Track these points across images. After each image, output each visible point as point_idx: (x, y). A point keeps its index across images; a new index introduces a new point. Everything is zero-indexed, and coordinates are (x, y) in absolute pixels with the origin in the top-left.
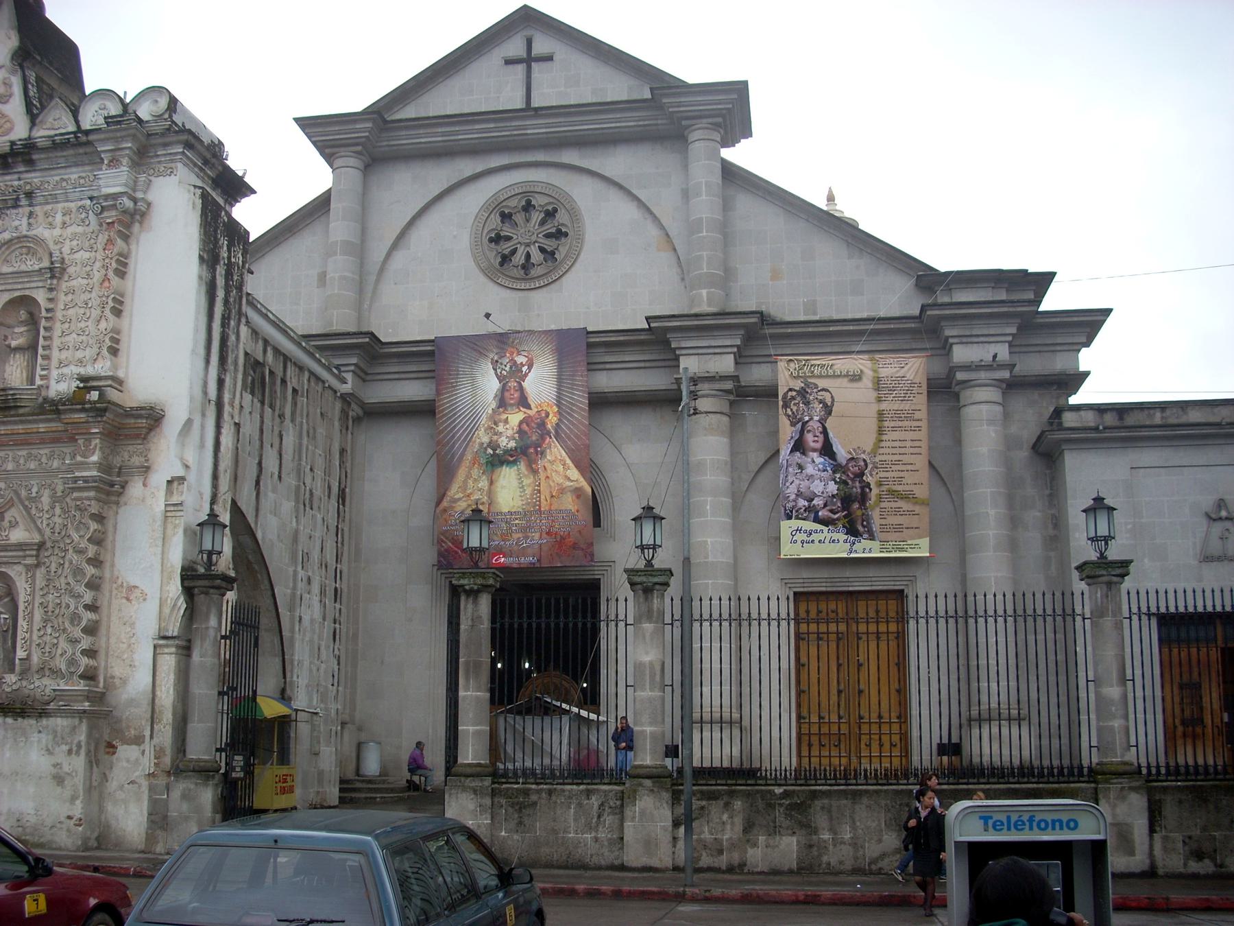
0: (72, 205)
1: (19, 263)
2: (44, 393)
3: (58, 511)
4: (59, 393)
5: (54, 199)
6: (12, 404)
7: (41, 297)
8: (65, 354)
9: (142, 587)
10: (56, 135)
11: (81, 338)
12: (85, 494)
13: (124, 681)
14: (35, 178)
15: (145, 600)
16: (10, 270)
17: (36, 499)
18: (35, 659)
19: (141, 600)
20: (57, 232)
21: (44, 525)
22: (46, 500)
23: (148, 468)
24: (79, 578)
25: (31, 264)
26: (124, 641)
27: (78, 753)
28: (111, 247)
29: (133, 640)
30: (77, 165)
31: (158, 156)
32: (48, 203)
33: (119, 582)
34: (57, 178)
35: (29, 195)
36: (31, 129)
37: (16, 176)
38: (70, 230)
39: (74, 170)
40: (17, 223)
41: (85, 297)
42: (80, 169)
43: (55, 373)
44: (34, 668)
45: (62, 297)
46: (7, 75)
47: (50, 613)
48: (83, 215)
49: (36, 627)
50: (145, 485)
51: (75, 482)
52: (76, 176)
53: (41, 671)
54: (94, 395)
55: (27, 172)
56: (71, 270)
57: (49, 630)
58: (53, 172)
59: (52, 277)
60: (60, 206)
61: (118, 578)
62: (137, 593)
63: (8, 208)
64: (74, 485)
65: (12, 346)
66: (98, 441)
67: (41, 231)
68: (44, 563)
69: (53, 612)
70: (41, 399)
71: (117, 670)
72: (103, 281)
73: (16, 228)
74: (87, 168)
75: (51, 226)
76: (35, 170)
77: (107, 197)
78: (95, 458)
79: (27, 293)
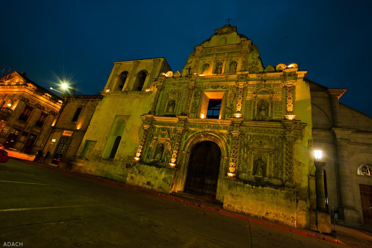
2: (272, 118)
3: (277, 143)
4: (276, 119)
13: (300, 184)
18: (273, 175)
27: (294, 201)
33: (296, 161)
36: (264, 70)
43: (274, 115)
49: (272, 167)
50: (302, 140)
53: (274, 178)
57: (276, 169)
70: (271, 119)
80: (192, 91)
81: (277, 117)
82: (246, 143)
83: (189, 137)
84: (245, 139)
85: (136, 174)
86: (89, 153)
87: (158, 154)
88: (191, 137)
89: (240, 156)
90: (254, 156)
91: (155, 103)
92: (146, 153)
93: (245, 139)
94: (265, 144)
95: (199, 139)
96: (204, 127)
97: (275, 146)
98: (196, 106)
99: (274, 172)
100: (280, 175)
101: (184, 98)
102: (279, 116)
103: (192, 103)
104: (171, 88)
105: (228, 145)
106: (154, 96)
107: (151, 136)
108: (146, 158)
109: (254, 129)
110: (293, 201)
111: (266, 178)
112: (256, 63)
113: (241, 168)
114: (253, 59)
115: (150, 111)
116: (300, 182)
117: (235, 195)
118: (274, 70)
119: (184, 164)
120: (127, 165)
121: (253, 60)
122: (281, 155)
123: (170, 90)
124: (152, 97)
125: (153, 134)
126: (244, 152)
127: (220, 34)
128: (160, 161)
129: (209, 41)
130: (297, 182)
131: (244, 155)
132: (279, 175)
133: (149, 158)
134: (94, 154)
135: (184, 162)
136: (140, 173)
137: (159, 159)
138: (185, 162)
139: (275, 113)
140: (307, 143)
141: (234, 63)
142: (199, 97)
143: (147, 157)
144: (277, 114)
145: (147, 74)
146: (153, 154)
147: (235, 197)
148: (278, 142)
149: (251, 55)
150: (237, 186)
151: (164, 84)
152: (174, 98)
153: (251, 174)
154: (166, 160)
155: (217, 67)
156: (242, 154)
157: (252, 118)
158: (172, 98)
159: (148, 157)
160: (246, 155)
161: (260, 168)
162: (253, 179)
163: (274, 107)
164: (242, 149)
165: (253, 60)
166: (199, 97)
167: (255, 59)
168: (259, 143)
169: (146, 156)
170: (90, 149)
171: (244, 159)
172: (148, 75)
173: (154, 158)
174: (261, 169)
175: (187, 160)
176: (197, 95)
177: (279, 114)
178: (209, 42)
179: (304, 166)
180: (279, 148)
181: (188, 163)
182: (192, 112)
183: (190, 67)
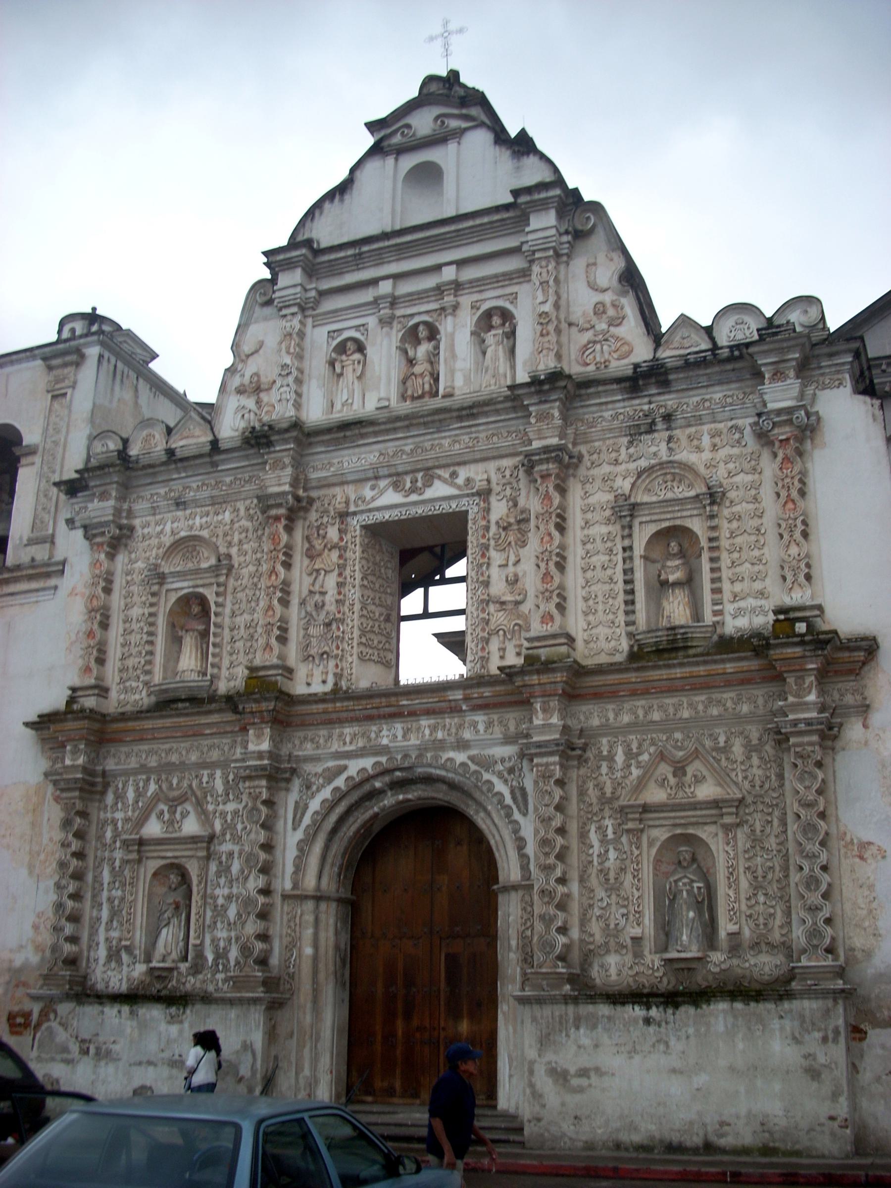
0: (721, 426)
1: (663, 492)
2: (719, 631)
3: (755, 761)
4: (739, 630)
5: (699, 420)
6: (681, 645)
7: (697, 526)
8: (738, 587)
9: (878, 842)
10: (689, 354)
11: (756, 568)
12: (806, 739)
13: (869, 954)
14: (669, 401)
16: (654, 499)
17: (726, 749)
18: (747, 933)
19: (879, 857)
20: (706, 455)
21: (740, 778)
22: (738, 749)
23: (868, 706)
24: (810, 835)
25: (682, 491)
26: (863, 906)
27: (835, 1040)
28: (789, 465)
29: (874, 905)
30: (720, 383)
31: (820, 368)
32: (690, 426)
33: (848, 838)
34: (698, 399)
35: (668, 418)
36: (655, 350)
37: (646, 400)
38: (722, 453)
39: (717, 388)
40: (653, 449)
41: (755, 522)
42: (725, 387)
43: (729, 608)
44: (746, 944)
45: (725, 525)
46: (615, 298)
47: (760, 879)
48: (737, 436)
49: (743, 897)
50: (865, 726)
51: (795, 725)
52: (720, 395)
53: (755, 946)
54: (801, 627)
55: (659, 394)
56: (732, 495)
57: (762, 899)
58: (691, 393)
59: (713, 503)
60: (705, 428)
61: (845, 834)
62: (873, 849)
63: (641, 434)
64: (793, 729)
65: (671, 580)
66: (813, 678)
67: (684, 455)
68: (747, 822)
69: (764, 877)
70: (715, 638)
71: (859, 942)
72: (786, 503)
73: (655, 454)
74: (733, 386)
75: (699, 449)
76: (670, 392)
77: (779, 412)
78: (812, 697)
79: (678, 522)
80: (289, 529)
81: (743, 623)
82: (608, 790)
83: (315, 805)
85: (68, 1062)
87: (164, 931)
90: (654, 851)
91: (90, 634)
93: (604, 769)
94: (699, 780)
96: (385, 733)
97: (746, 783)
98: (322, 616)
99: (750, 916)
100: (781, 927)
101: (252, 576)
102: (753, 610)
103: (303, 603)
104: (168, 528)
105: (517, 816)
106: (80, 589)
107: (109, 834)
108: (102, 961)
110: (830, 1044)
111: (717, 957)
112: (611, 312)
113: (595, 927)
114: (593, 287)
115: (74, 690)
117: (572, 1070)
119: (310, 962)
120: (11, 1017)
121: (597, 297)
122: (776, 822)
123: (167, 540)
124: (72, 593)
125: (114, 822)
126: (604, 841)
127: (400, 151)
128: (183, 967)
131: (603, 856)
132: (776, 927)
133: (120, 962)
135: (309, 951)
136: (86, 1052)
137: (174, 955)
138: (316, 946)
139: (735, 597)
141: (496, 320)
142: (335, 555)
143: (109, 958)
144: (742, 604)
146: (138, 933)
147: (575, 1082)
148: (761, 758)
149: (579, 264)
150: (577, 1028)
151: (126, 506)
152: (194, 587)
153: (646, 953)
154: (210, 957)
155: (411, 353)
156: (597, 849)
157: (625, 645)
158: (185, 584)
159: (114, 955)
160: (612, 854)
161: (688, 910)
162: (660, 974)
163: (725, 560)
164: (593, 828)
165: (597, 297)
166: (335, 555)
168: (672, 781)
169: (102, 953)
171: (607, 880)
172: (23, 461)
173: (148, 959)
174: (691, 914)
175: (322, 935)
176: (318, 544)
177: (751, 602)
180: (767, 786)
181: (331, 952)
182: (308, 658)
183: (257, 374)
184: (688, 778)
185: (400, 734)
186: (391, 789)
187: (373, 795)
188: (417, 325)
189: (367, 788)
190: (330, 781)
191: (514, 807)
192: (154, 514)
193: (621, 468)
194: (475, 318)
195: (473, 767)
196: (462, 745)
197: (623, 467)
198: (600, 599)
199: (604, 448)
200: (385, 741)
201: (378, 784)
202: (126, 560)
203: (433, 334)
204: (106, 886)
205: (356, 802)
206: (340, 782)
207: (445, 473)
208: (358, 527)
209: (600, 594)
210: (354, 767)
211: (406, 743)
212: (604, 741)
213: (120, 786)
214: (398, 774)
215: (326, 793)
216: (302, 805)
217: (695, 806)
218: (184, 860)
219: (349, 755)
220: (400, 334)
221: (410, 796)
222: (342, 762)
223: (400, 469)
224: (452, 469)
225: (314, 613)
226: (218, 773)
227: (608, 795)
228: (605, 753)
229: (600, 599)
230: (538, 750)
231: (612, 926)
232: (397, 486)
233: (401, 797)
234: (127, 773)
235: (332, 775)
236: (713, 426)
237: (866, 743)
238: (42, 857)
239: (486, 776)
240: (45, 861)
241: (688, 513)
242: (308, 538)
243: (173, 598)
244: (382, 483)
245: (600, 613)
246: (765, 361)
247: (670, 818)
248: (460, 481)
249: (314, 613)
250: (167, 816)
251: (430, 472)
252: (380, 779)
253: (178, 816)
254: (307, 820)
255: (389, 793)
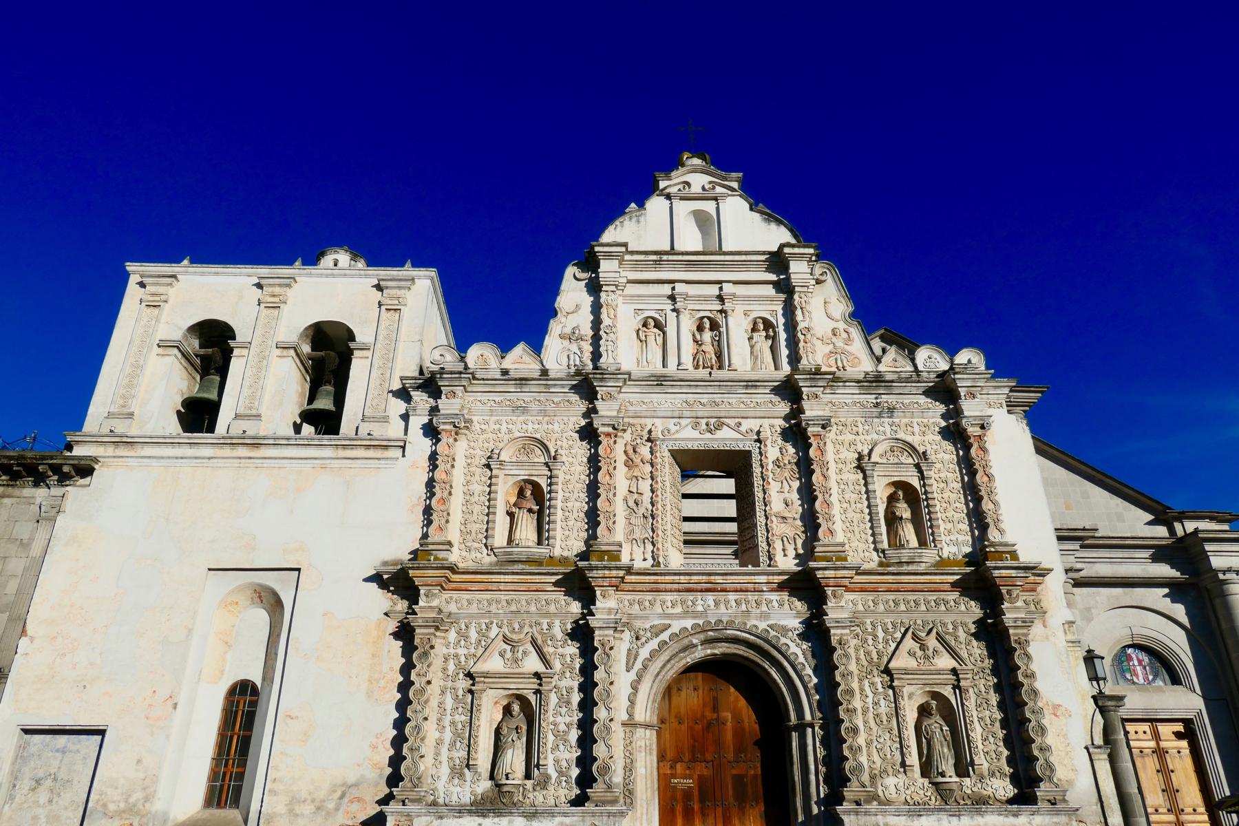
10: (901, 372)
15: (1070, 716)
26: (1062, 749)
29: (1069, 749)
51: (1015, 622)
57: (992, 740)
60: (915, 420)
83: (644, 653)
84: (870, 642)
86: (50, 801)
87: (510, 752)
88: (653, 655)
89: (865, 711)
92: (444, 757)
93: (870, 642)
95: (685, 657)
104: (504, 429)
109: (892, 597)
116: (1071, 776)
118: (912, 369)
121: (835, 325)
129: (642, 219)
130: (1062, 777)
134: (105, 805)
140: (1060, 633)
145: (352, 345)
155: (698, 337)
158: (522, 472)
160: (882, 702)
167: (837, 321)
168: (919, 653)
169: (445, 770)
170: (55, 779)
178: (642, 223)
179: (1070, 716)
184: (930, 653)
185: (712, 603)
186: (701, 645)
187: (690, 647)
188: (702, 318)
189: (686, 642)
190: (657, 635)
191: (806, 664)
192: (491, 415)
193: (858, 438)
194: (747, 322)
195: (773, 633)
196: (764, 616)
197: (862, 437)
198: (856, 523)
199: (848, 424)
200: (700, 608)
201: (695, 641)
202: (466, 446)
203: (714, 326)
204: (449, 712)
205: (677, 653)
206: (665, 636)
207: (732, 422)
208: (666, 451)
209: (854, 520)
210: (676, 626)
211: (717, 611)
212: (868, 621)
213: (463, 627)
214: (711, 633)
215: (654, 644)
216: (634, 652)
217: (939, 672)
218: (525, 691)
219: (670, 616)
220: (690, 322)
221: (716, 651)
222: (667, 622)
223: (700, 414)
224: (737, 420)
225: (635, 508)
226: (557, 623)
227: (875, 660)
228: (870, 630)
229: (856, 523)
230: (837, 625)
231: (889, 756)
232: (696, 426)
233: (709, 652)
234: (471, 616)
235: (657, 631)
236: (920, 420)
237: (1047, 638)
238: (382, 683)
239: (783, 640)
240: (384, 688)
241: (910, 474)
242: (625, 452)
243: (512, 480)
244: (684, 422)
245: (856, 533)
246: (961, 385)
247: (923, 679)
248: (743, 429)
249: (635, 508)
250: (509, 655)
251: (722, 420)
252: (697, 636)
253: (520, 655)
254: (638, 665)
255: (700, 647)
